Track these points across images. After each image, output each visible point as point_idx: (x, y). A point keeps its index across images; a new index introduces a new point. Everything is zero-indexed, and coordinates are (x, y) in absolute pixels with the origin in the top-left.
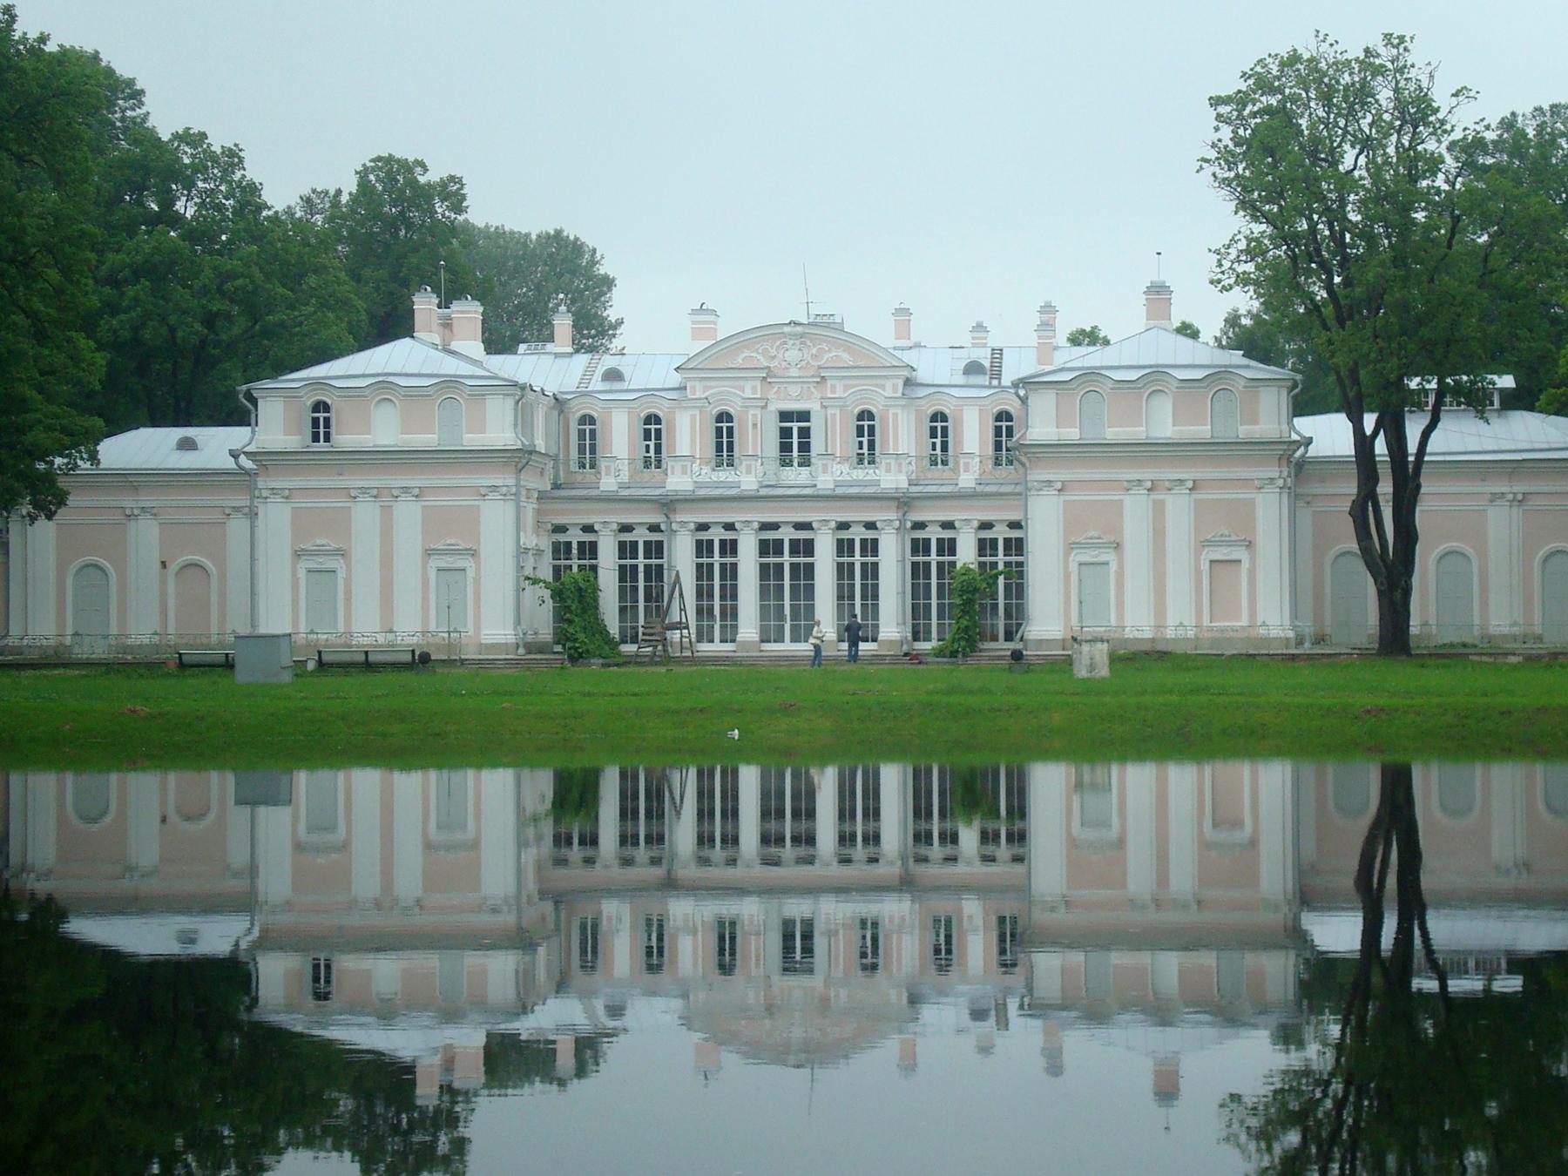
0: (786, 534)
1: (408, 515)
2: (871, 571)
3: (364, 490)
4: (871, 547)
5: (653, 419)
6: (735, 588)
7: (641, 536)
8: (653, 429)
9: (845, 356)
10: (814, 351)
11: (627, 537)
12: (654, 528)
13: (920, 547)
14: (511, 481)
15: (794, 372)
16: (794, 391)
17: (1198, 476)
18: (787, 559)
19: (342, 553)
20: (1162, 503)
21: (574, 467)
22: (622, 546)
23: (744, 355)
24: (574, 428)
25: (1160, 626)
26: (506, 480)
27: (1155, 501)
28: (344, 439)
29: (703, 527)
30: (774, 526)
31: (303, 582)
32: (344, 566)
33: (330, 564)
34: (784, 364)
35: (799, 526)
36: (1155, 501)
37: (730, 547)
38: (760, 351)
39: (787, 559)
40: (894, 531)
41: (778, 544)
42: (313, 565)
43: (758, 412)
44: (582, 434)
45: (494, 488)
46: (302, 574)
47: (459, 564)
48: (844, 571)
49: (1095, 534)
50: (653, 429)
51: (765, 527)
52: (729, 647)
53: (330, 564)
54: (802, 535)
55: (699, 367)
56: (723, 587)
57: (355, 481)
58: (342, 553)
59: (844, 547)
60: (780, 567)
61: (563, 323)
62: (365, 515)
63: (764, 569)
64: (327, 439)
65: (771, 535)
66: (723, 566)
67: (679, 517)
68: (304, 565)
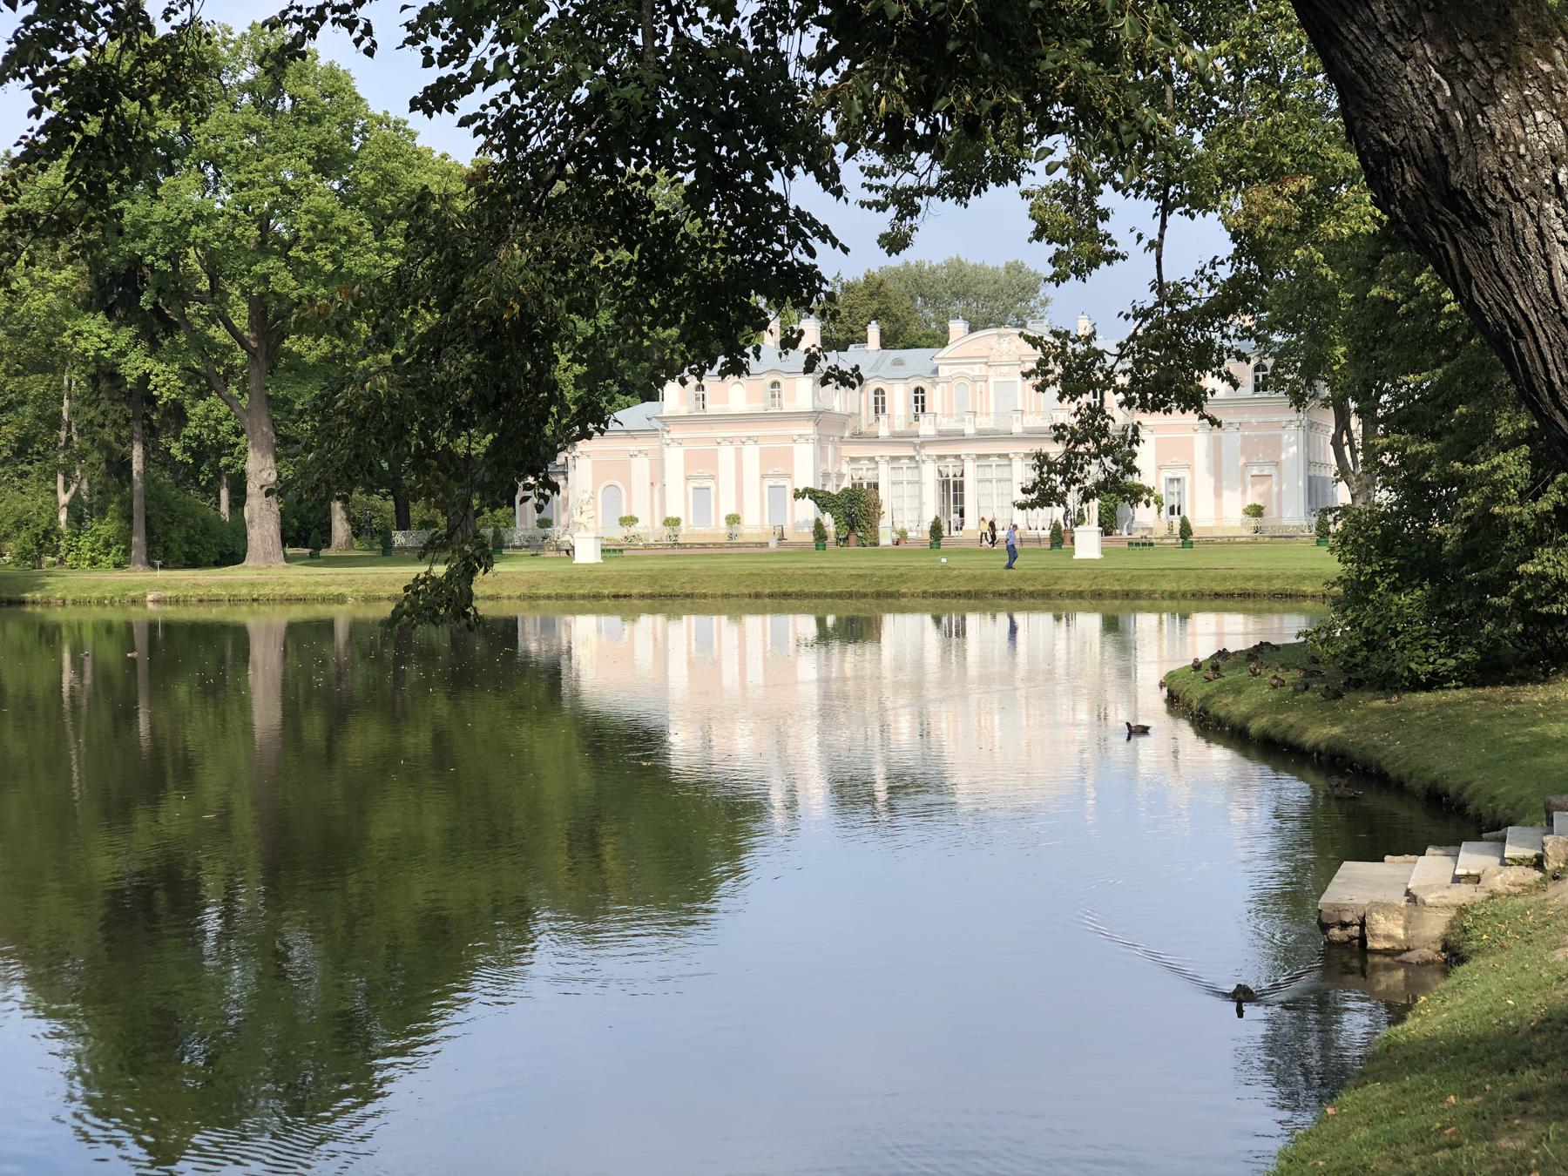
1: (751, 453)
3: (724, 439)
5: (918, 390)
6: (962, 496)
8: (919, 396)
12: (912, 458)
14: (811, 431)
15: (1005, 358)
16: (1005, 369)
17: (1240, 420)
19: (713, 477)
20: (1220, 438)
21: (872, 420)
24: (872, 396)
25: (1219, 517)
26: (809, 429)
27: (1215, 437)
29: (941, 457)
30: (988, 456)
36: (1215, 437)
42: (697, 485)
44: (876, 399)
45: (800, 436)
47: (782, 483)
49: (1175, 459)
50: (919, 396)
51: (979, 456)
52: (961, 533)
53: (706, 484)
56: (955, 496)
57: (720, 432)
58: (713, 477)
61: (873, 331)
62: (726, 454)
66: (955, 483)
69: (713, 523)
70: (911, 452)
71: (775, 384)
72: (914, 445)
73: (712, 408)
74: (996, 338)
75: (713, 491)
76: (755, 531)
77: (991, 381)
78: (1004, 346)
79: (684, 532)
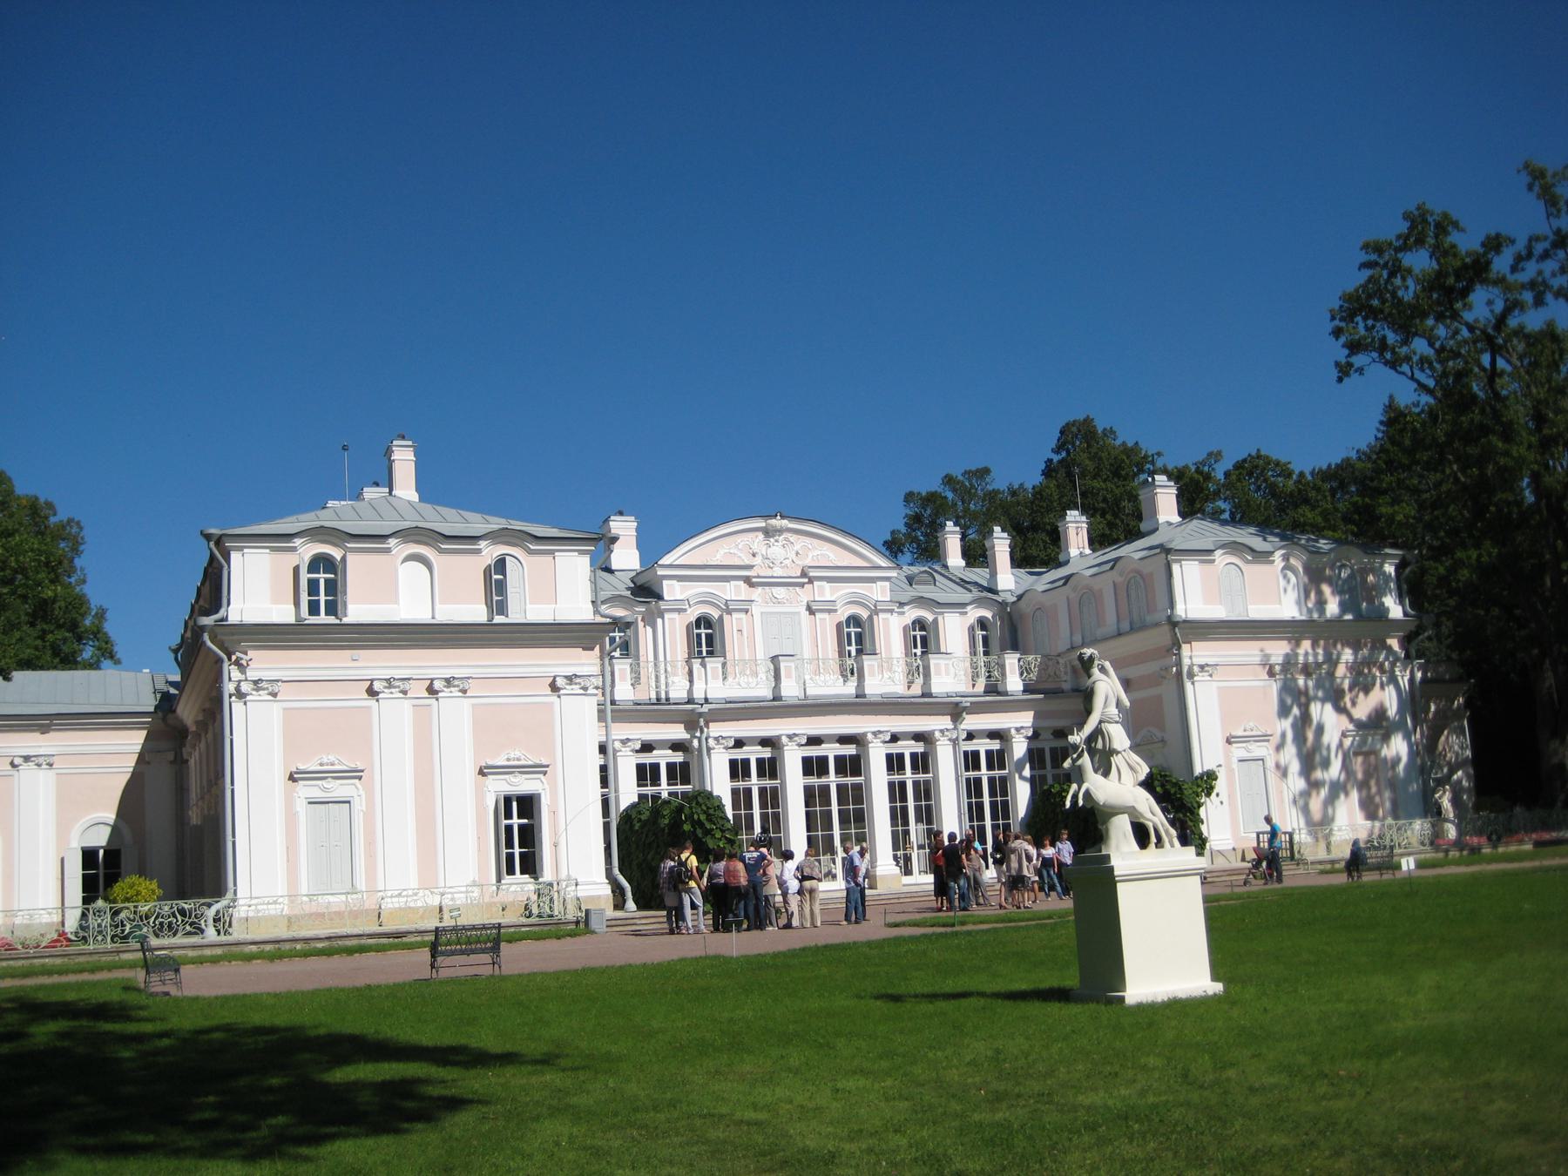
0: (831, 751)
2: (926, 792)
4: (922, 762)
7: (663, 757)
9: (832, 556)
10: (798, 547)
11: (647, 759)
12: (676, 746)
13: (972, 760)
15: (778, 571)
16: (780, 592)
18: (832, 779)
22: (641, 769)
23: (722, 552)
28: (357, 611)
31: (302, 819)
32: (362, 792)
33: (339, 789)
34: (767, 561)
35: (844, 740)
37: (770, 768)
38: (740, 547)
39: (832, 779)
40: (949, 743)
41: (823, 761)
43: (742, 615)
46: (301, 806)
47: (523, 785)
48: (897, 792)
54: (850, 750)
55: (675, 563)
58: (355, 774)
59: (895, 763)
60: (825, 790)
63: (809, 793)
64: (332, 609)
65: (814, 752)
67: (716, 729)
68: (305, 790)
69: (361, 884)
70: (678, 732)
71: (501, 564)
72: (692, 722)
73: (357, 611)
74: (761, 536)
75: (359, 805)
76: (273, 910)
77: (756, 610)
78: (777, 549)
79: (240, 912)
